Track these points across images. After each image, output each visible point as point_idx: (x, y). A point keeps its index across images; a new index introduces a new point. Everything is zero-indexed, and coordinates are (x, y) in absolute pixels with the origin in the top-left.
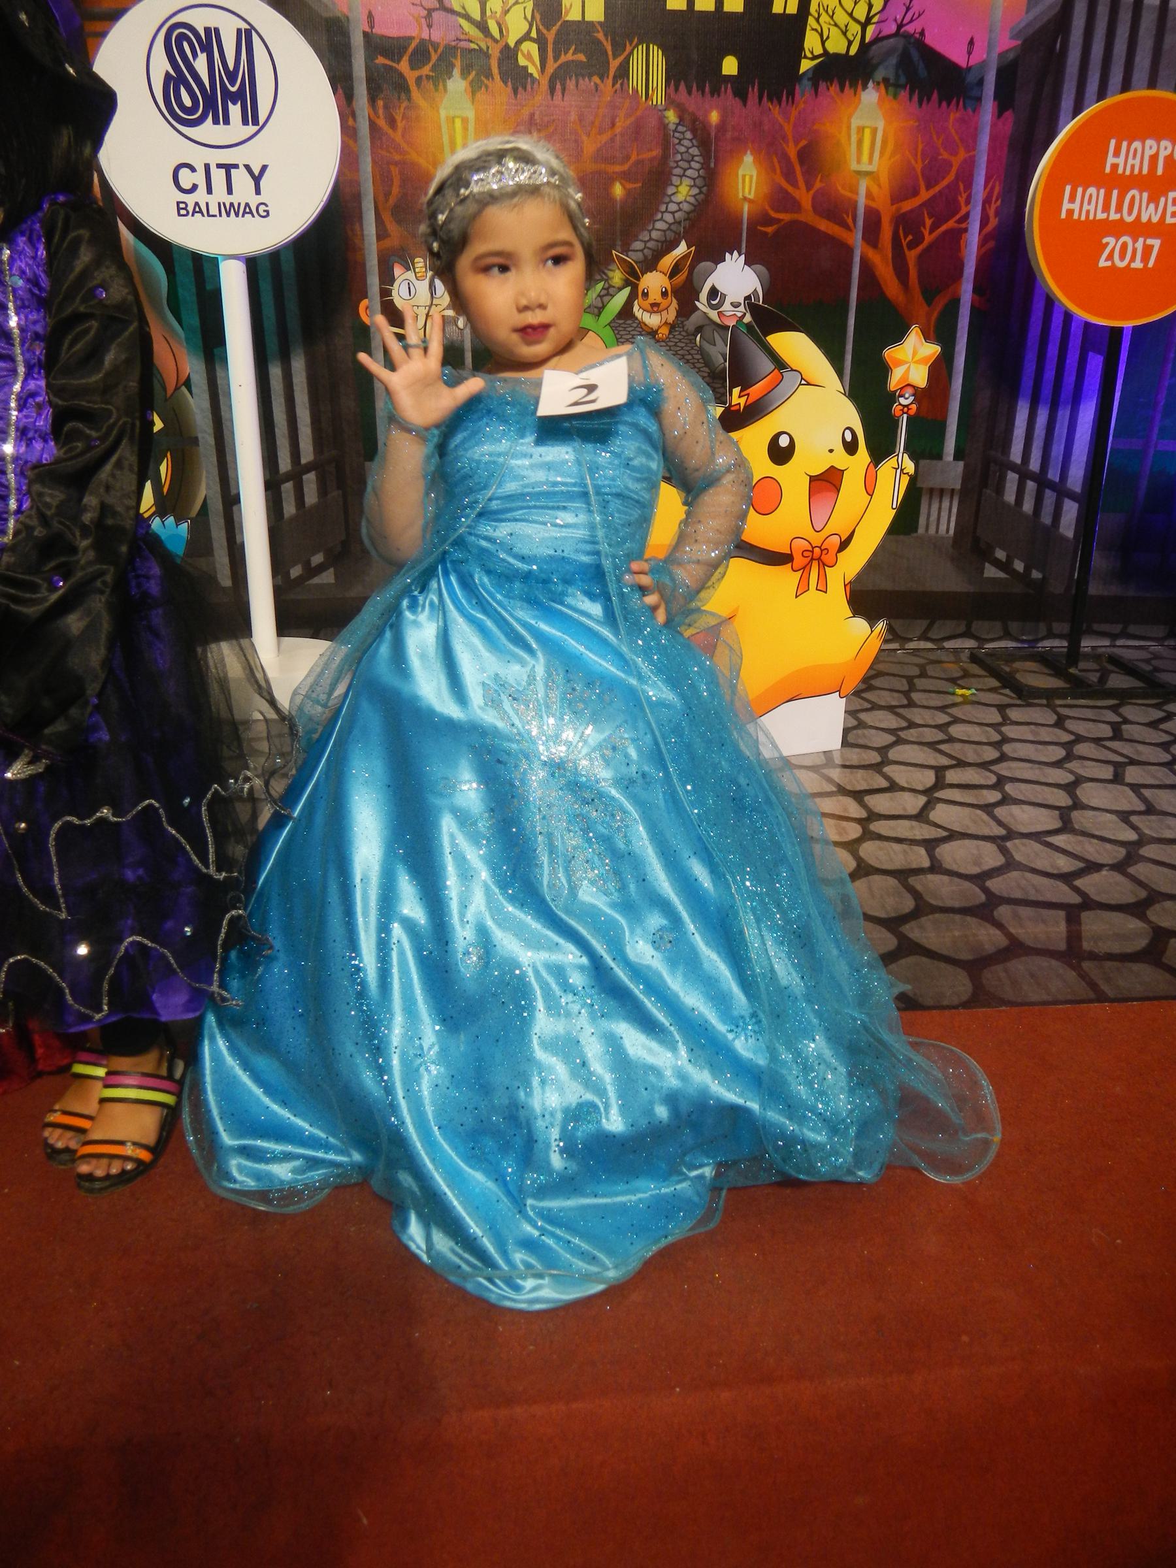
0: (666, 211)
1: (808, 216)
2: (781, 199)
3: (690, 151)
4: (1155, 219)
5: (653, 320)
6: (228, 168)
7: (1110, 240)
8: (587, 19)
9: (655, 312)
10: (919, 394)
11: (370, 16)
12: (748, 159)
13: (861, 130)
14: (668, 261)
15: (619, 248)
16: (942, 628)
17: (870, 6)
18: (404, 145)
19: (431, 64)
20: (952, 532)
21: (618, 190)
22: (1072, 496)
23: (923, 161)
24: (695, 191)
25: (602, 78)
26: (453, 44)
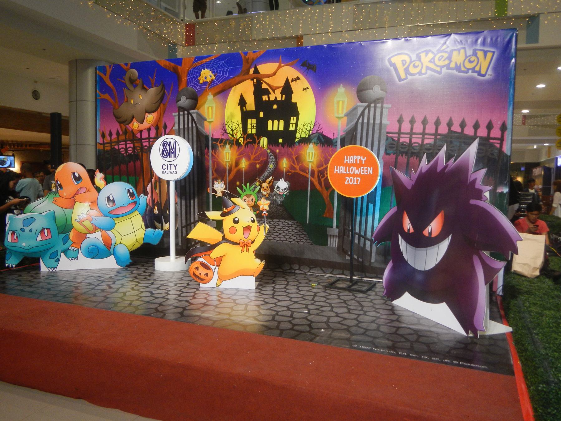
1: (298, 171)
2: (292, 167)
4: (358, 173)
5: (265, 193)
6: (171, 165)
7: (348, 178)
10: (268, 211)
11: (213, 135)
12: (285, 159)
13: (309, 153)
14: (268, 180)
16: (336, 271)
17: (310, 127)
20: (337, 246)
21: (258, 166)
22: (369, 240)
23: (324, 158)
24: (274, 166)
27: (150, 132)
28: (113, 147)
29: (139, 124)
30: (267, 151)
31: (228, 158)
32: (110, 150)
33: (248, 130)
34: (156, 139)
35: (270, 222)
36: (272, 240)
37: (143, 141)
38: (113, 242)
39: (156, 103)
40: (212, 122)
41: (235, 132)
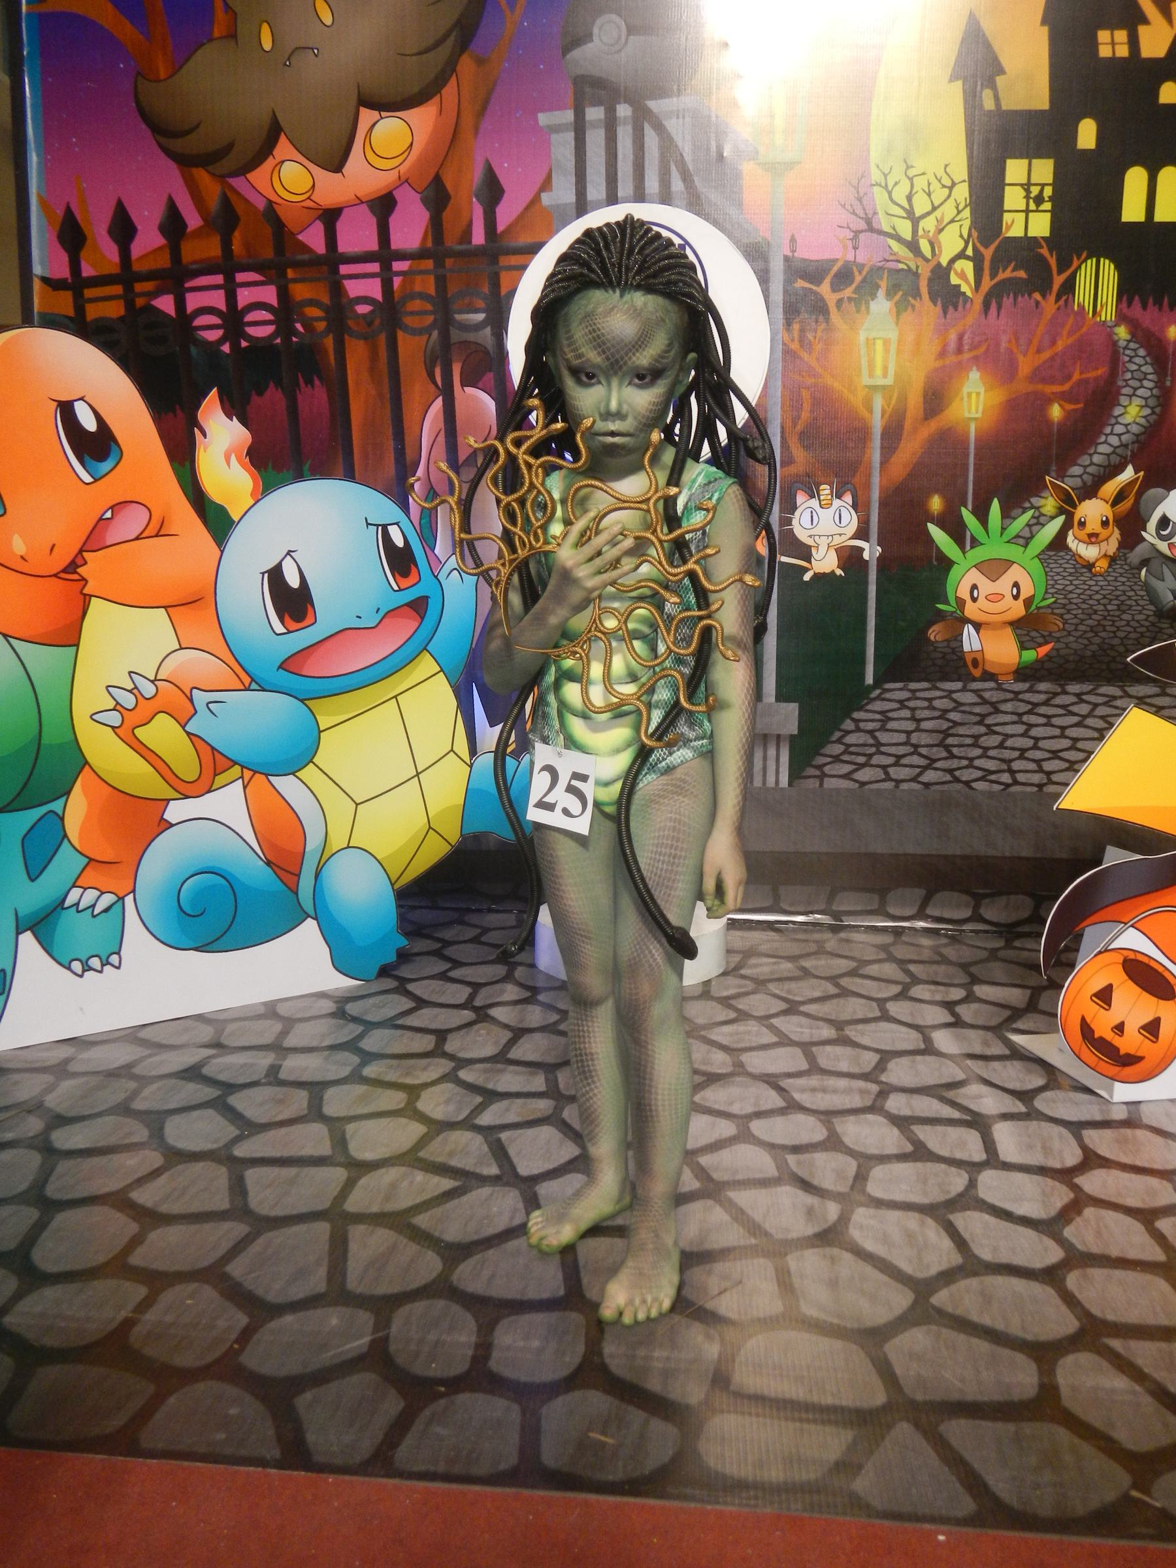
0: (1112, 433)
3: (1143, 369)
5: (1089, 552)
8: (1030, 235)
9: (1092, 543)
11: (793, 240)
14: (1111, 488)
15: (1053, 474)
18: (819, 370)
19: (854, 285)
21: (1056, 412)
24: (1147, 411)
25: (1044, 296)
26: (880, 264)
27: (394, 221)
28: (140, 302)
29: (318, 171)
30: (1110, 335)
31: (879, 371)
32: (122, 319)
33: (1007, 217)
34: (429, 264)
35: (1115, 698)
36: (977, 785)
37: (344, 269)
38: (313, 843)
39: (427, 50)
40: (790, 165)
41: (929, 224)
